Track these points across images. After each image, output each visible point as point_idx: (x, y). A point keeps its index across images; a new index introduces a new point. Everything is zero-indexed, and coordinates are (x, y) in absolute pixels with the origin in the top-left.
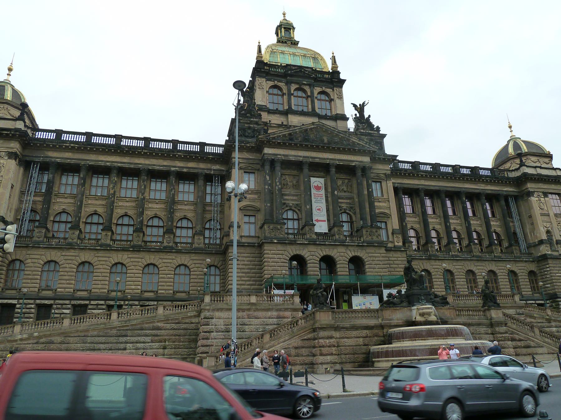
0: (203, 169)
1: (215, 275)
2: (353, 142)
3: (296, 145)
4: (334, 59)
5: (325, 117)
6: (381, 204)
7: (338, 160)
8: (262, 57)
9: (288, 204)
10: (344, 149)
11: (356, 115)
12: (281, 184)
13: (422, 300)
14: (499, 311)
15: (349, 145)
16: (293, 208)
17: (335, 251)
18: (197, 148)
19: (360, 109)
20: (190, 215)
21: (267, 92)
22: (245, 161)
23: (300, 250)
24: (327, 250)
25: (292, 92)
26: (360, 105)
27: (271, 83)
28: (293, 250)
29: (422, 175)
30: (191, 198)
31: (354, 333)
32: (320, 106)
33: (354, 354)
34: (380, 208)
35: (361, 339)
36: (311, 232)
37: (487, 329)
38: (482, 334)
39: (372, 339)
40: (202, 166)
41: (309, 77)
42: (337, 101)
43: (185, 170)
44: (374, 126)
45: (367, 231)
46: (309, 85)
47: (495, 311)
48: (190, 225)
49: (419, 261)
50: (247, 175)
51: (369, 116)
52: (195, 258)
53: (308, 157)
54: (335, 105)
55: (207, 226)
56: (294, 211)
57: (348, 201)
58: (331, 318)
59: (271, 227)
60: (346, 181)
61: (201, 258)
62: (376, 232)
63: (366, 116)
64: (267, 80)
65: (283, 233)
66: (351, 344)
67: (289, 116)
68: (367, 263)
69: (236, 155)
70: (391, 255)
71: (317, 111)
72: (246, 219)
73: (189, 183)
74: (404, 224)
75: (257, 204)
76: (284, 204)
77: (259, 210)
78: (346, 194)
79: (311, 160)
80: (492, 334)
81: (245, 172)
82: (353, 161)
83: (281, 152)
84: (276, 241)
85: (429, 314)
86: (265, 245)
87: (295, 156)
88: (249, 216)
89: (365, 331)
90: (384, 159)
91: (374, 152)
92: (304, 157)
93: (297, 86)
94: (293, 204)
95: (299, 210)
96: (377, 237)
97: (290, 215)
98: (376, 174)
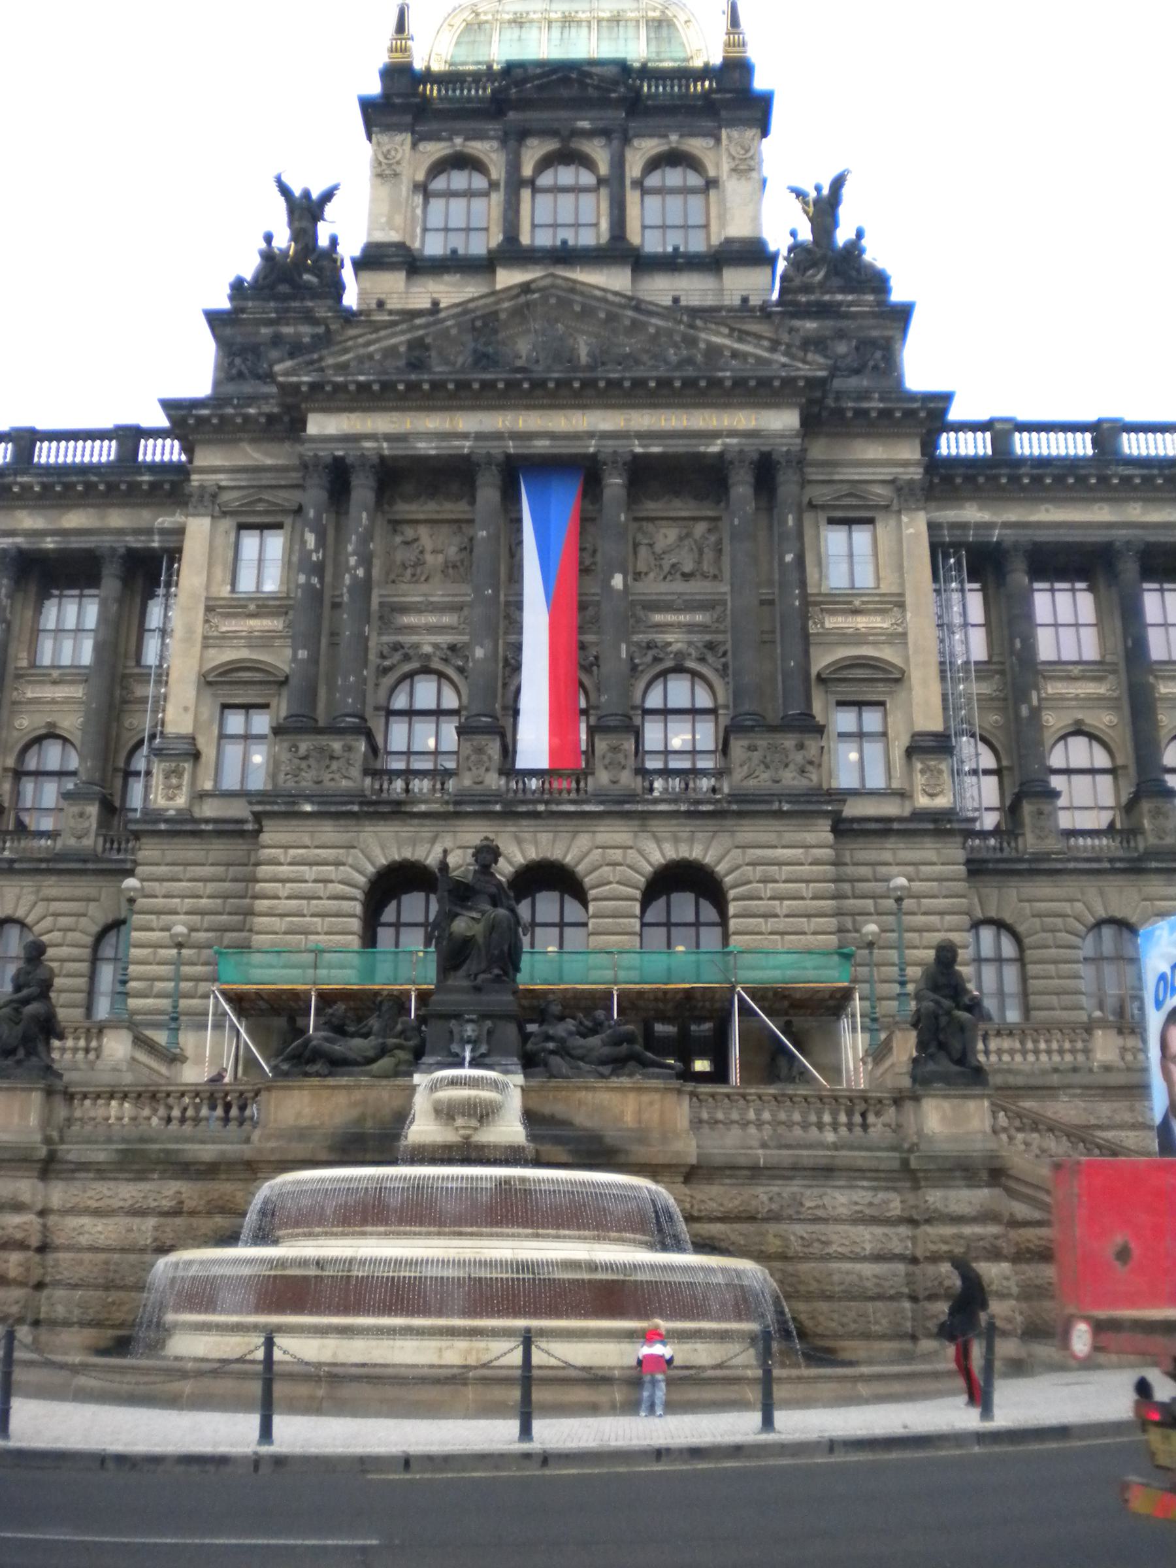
0: (121, 532)
2: (714, 351)
3: (438, 386)
5: (672, 263)
6: (861, 623)
7: (641, 436)
8: (405, 50)
9: (416, 646)
10: (664, 383)
11: (793, 234)
12: (366, 560)
13: (465, 1041)
14: (972, 1105)
15: (690, 361)
16: (436, 664)
17: (583, 841)
18: (104, 452)
20: (71, 722)
21: (423, 189)
22: (243, 480)
23: (414, 842)
24: (544, 837)
25: (527, 171)
26: (818, 189)
27: (435, 150)
28: (384, 845)
29: (1126, 480)
30: (87, 656)
31: (127, 1192)
32: (651, 222)
33: (107, 1288)
34: (859, 638)
35: (151, 1222)
36: (479, 763)
37: (881, 1195)
38: (837, 1220)
39: (194, 1221)
40: (117, 519)
41: (603, 102)
42: (733, 187)
43: (49, 544)
45: (752, 748)
46: (604, 133)
47: (946, 1105)
48: (74, 763)
49: (1084, 881)
50: (250, 542)
52: (53, 892)
53: (498, 436)
54: (722, 202)
56: (441, 675)
57: (699, 618)
58: (33, 1120)
59: (303, 747)
60: (700, 528)
61: (78, 892)
62: (801, 747)
63: (843, 236)
65: (355, 772)
66: (102, 1241)
68: (732, 893)
70: (887, 856)
71: (634, 236)
72: (235, 722)
73: (81, 596)
74: (1024, 711)
75: (281, 659)
76: (397, 647)
77: (284, 682)
78: (697, 588)
79: (511, 447)
80: (912, 1222)
81: (241, 527)
82: (715, 435)
84: (308, 808)
85: (484, 1113)
86: (267, 824)
88: (247, 707)
89: (173, 1188)
90: (886, 414)
91: (811, 383)
92: (480, 436)
93: (551, 145)
94: (436, 646)
95: (461, 670)
96: (803, 771)
98: (845, 489)
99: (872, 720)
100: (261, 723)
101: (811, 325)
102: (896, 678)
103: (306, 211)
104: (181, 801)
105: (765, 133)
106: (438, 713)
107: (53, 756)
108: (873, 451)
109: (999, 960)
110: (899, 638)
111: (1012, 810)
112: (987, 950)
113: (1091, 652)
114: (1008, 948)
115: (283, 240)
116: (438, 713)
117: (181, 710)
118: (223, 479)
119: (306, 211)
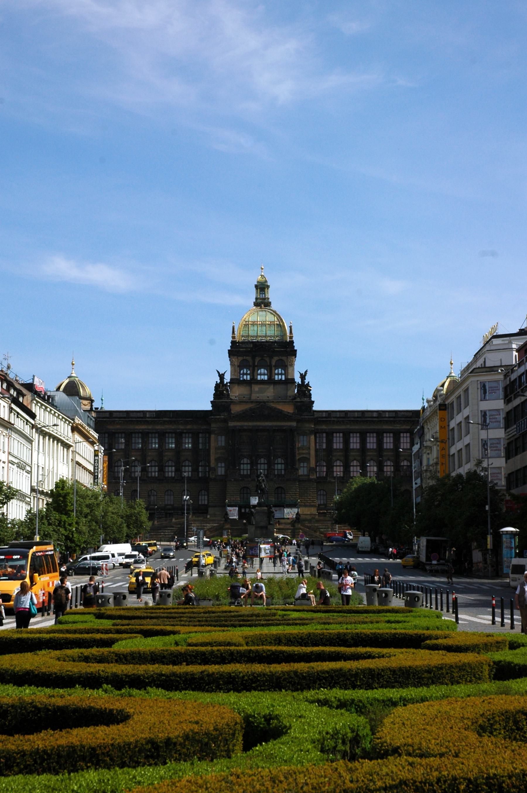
1: (205, 495)
4: (291, 327)
8: (235, 337)
19: (303, 377)
21: (239, 366)
25: (256, 364)
40: (195, 427)
43: (185, 431)
44: (311, 390)
50: (219, 437)
51: (309, 382)
55: (200, 464)
64: (239, 356)
67: (253, 385)
69: (213, 425)
72: (219, 465)
83: (238, 424)
87: (246, 426)
93: (260, 359)
97: (245, 460)
99: (305, 465)
100: (223, 465)
101: (299, 404)
102: (309, 459)
103: (222, 376)
104: (214, 477)
105: (296, 357)
106: (247, 464)
107: (187, 463)
108: (307, 425)
109: (323, 495)
110: (309, 454)
111: (327, 472)
112: (322, 493)
113: (341, 447)
114: (325, 493)
115: (219, 381)
116: (247, 464)
117: (213, 464)
118: (216, 429)
119: (222, 376)
